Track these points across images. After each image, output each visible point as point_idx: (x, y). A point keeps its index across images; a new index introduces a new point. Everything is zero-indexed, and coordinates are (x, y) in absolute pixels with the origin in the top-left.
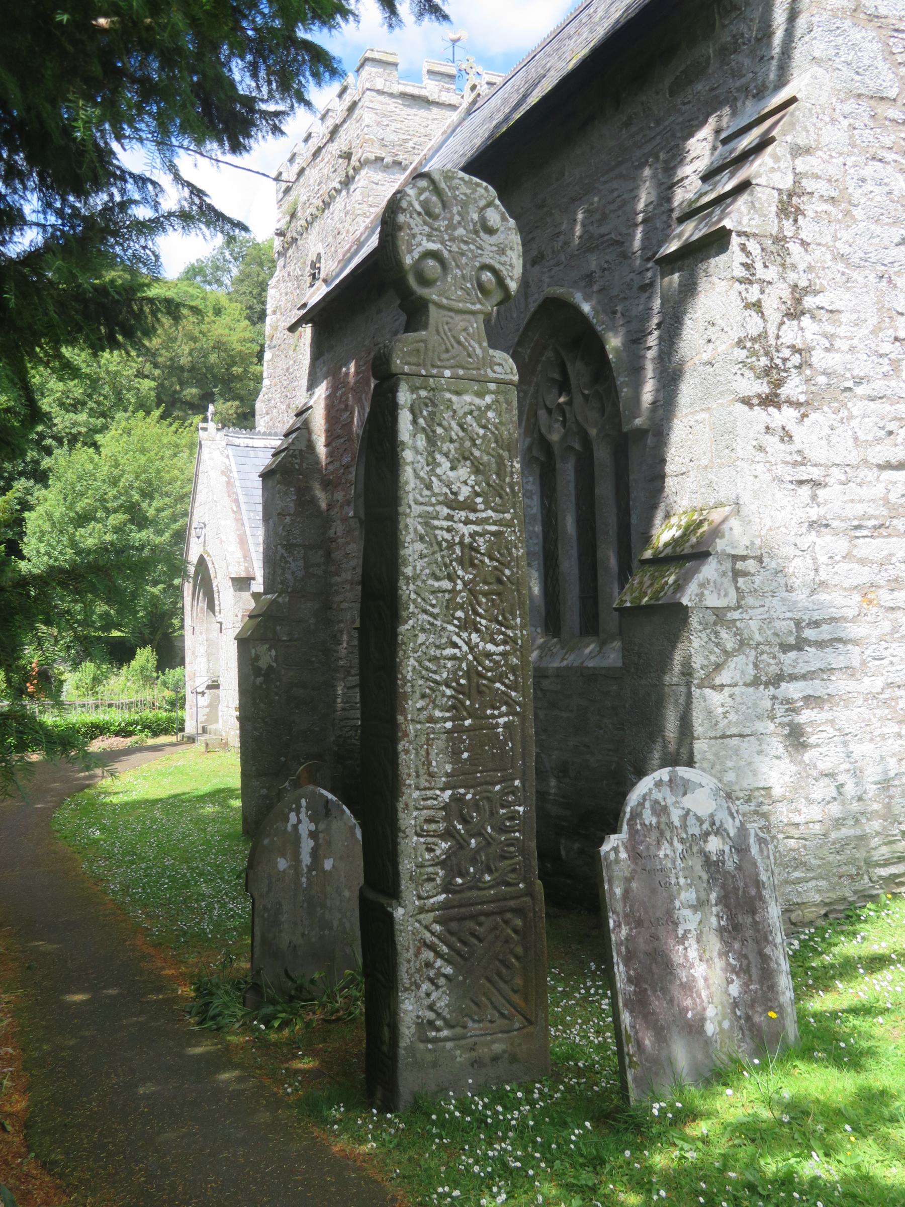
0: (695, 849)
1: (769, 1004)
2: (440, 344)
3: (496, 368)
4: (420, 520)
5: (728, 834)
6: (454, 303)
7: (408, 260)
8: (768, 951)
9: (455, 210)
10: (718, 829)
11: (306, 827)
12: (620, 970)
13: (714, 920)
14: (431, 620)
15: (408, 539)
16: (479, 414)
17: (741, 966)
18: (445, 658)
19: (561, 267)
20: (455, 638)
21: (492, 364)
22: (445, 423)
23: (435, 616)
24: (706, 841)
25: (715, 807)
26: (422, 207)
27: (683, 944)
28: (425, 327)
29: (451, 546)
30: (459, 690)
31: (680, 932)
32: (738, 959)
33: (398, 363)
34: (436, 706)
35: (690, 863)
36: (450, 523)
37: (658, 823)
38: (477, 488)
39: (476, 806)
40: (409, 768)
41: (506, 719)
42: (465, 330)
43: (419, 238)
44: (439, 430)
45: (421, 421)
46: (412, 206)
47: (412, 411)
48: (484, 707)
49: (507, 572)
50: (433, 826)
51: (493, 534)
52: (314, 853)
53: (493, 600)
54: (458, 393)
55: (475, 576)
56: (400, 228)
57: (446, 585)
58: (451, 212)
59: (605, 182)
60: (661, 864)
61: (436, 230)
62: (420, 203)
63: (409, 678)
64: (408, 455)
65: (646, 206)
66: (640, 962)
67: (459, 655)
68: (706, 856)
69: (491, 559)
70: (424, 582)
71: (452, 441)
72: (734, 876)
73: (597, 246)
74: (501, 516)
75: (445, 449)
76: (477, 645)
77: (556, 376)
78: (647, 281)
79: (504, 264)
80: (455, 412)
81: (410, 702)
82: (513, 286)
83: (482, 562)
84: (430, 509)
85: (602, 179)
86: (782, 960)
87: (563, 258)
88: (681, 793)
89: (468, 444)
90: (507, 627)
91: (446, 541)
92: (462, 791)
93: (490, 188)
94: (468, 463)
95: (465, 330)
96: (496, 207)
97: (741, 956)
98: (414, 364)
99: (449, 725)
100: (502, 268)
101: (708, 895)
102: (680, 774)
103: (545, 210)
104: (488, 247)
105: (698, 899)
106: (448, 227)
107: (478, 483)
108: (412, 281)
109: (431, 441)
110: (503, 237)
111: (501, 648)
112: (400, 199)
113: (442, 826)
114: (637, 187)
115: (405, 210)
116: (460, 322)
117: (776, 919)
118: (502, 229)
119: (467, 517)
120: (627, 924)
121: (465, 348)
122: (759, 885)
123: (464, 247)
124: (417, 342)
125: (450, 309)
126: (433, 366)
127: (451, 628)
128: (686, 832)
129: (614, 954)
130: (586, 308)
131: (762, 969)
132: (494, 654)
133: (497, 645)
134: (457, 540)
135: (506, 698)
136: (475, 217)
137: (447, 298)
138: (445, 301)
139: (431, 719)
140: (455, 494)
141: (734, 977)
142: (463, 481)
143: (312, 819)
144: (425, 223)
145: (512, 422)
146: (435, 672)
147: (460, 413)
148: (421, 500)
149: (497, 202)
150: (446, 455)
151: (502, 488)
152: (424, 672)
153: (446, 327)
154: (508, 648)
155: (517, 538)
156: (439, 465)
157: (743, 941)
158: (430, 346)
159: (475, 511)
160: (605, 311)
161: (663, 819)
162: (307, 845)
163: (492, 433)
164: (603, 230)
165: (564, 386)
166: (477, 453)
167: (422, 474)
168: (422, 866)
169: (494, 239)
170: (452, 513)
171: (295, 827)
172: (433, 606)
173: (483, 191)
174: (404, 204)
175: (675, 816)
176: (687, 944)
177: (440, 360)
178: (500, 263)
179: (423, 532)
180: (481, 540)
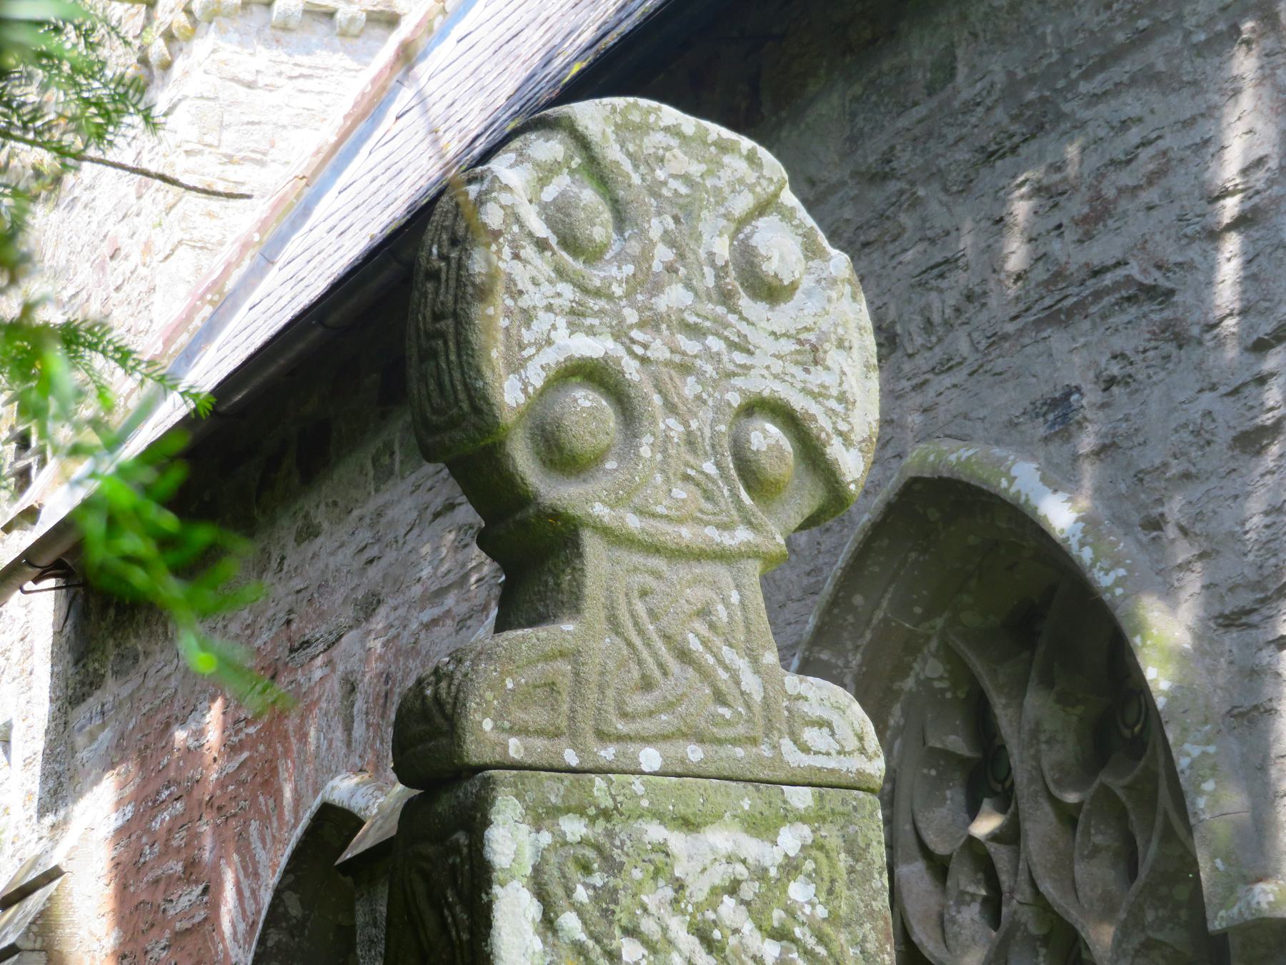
3: (811, 735)
7: (510, 394)
9: (655, 228)
19: (959, 376)
21: (795, 724)
22: (648, 926)
26: (550, 222)
28: (573, 604)
33: (486, 732)
42: (704, 613)
43: (543, 321)
45: (570, 922)
46: (518, 220)
54: (688, 824)
56: (483, 293)
58: (643, 232)
59: (1096, 98)
61: (597, 293)
62: (544, 207)
65: (1245, 172)
73: (1081, 305)
77: (957, 743)
78: (1268, 419)
79: (818, 395)
80: (680, 886)
82: (852, 465)
85: (1084, 87)
87: (964, 347)
93: (764, 153)
96: (787, 215)
98: (540, 733)
100: (814, 408)
103: (893, 186)
104: (768, 345)
106: (633, 285)
108: (523, 459)
110: (812, 306)
112: (480, 201)
114: (1211, 113)
115: (496, 234)
116: (688, 587)
118: (807, 282)
123: (690, 346)
124: (547, 658)
125: (654, 549)
130: (1060, 515)
136: (722, 248)
138: (633, 523)
144: (561, 273)
145: (872, 914)
147: (699, 890)
149: (789, 198)
158: (591, 673)
160: (1120, 521)
163: (807, 953)
164: (1099, 252)
165: (985, 777)
169: (784, 316)
173: (742, 166)
174: (493, 216)
177: (624, 715)
178: (805, 391)
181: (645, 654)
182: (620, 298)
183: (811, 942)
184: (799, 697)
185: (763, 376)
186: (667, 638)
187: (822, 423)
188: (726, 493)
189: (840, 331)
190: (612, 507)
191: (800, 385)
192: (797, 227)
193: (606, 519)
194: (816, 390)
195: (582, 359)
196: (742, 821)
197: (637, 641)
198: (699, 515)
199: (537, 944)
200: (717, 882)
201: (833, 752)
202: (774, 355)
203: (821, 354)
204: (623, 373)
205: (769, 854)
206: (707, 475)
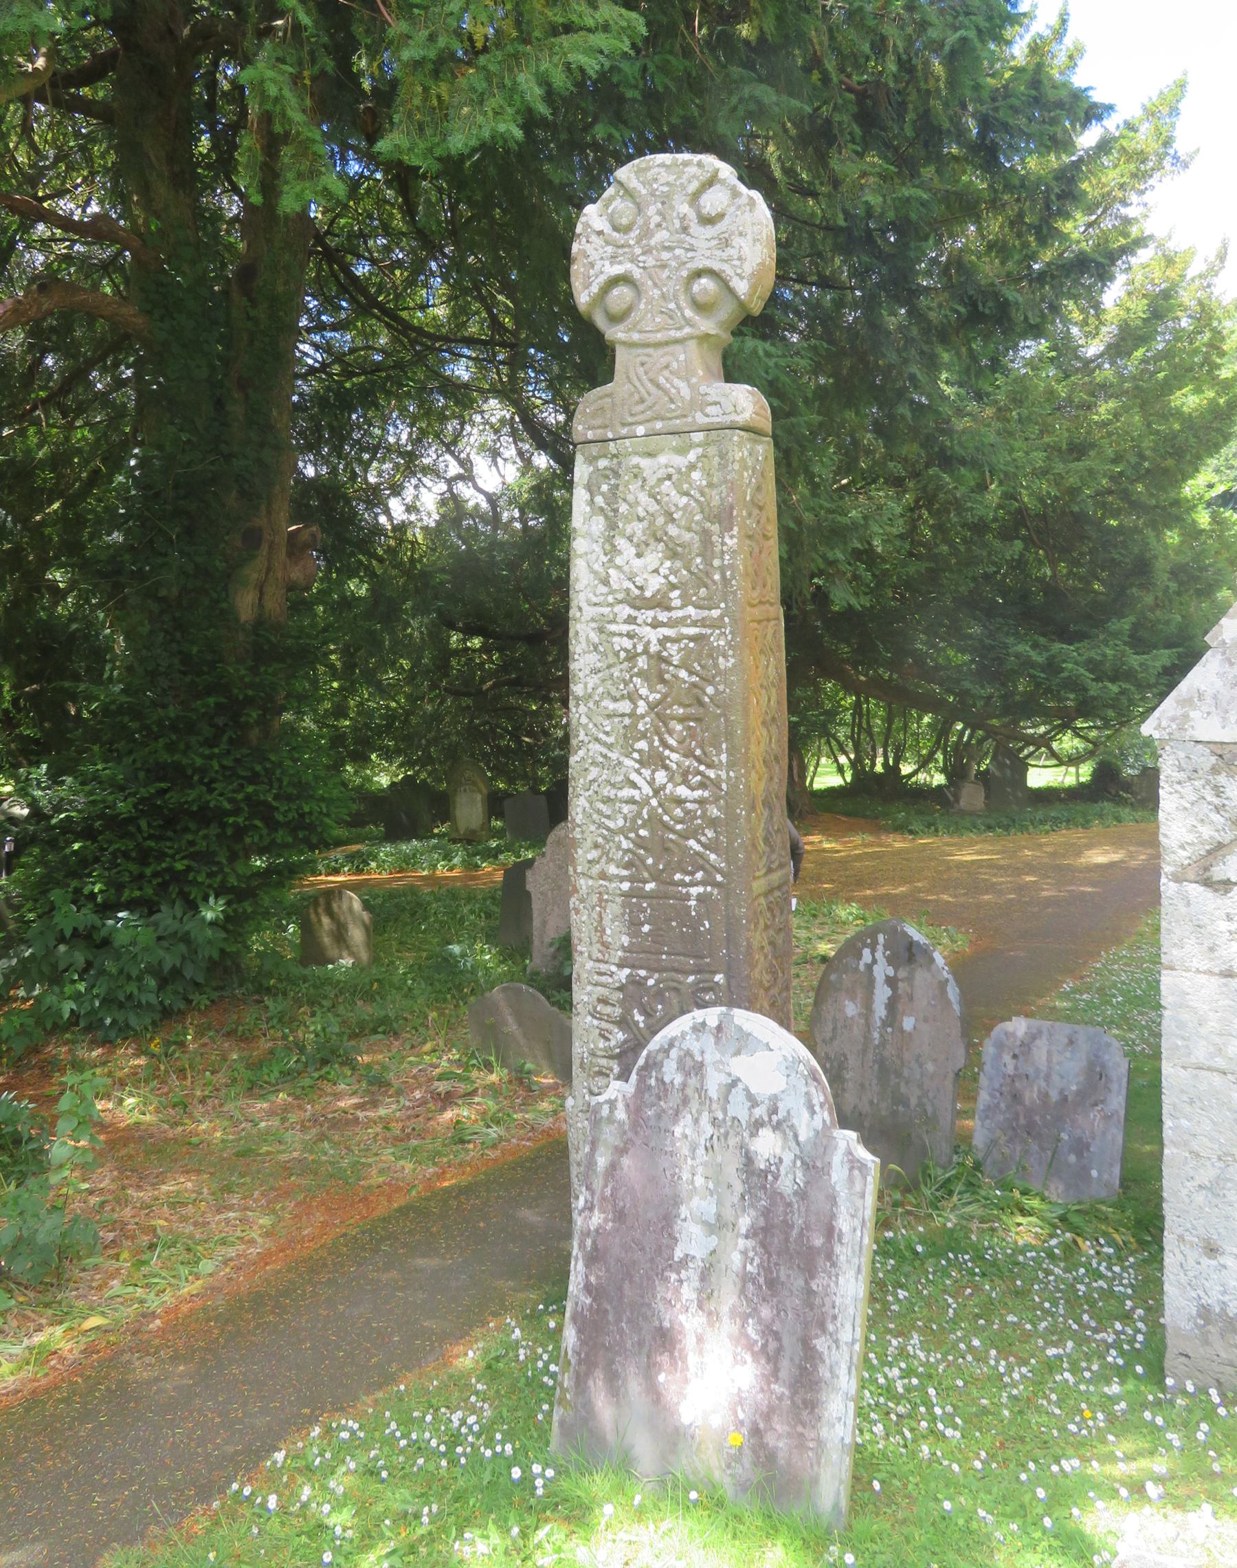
0: (733, 1141)
1: (800, 1429)
2: (632, 395)
4: (594, 625)
5: (796, 1136)
7: (583, 299)
8: (821, 1344)
9: (651, 210)
10: (779, 1123)
11: (882, 970)
12: (578, 1269)
13: (736, 1258)
14: (605, 751)
15: (578, 650)
16: (679, 478)
17: (765, 1346)
18: (621, 801)
20: (634, 777)
22: (630, 498)
23: (610, 747)
24: (754, 1134)
25: (784, 1086)
27: (679, 1273)
28: (609, 377)
29: (632, 657)
30: (640, 843)
31: (678, 1254)
32: (763, 1334)
34: (609, 860)
35: (719, 1159)
36: (632, 627)
37: (684, 1085)
38: (672, 578)
39: (659, 995)
40: (580, 931)
41: (701, 889)
44: (623, 508)
47: (589, 487)
48: (671, 868)
49: (710, 690)
50: (608, 1010)
51: (692, 638)
52: (892, 1005)
53: (690, 728)
54: (650, 455)
55: (665, 696)
57: (625, 706)
60: (673, 1144)
61: (623, 246)
63: (578, 821)
64: (579, 545)
66: (607, 1271)
67: (637, 798)
68: (749, 1160)
69: (691, 673)
70: (597, 703)
71: (640, 520)
72: (790, 1205)
74: (706, 613)
75: (629, 531)
76: (664, 787)
81: (580, 851)
83: (675, 676)
84: (606, 610)
86: (843, 1371)
88: (732, 1050)
89: (660, 520)
90: (709, 766)
91: (626, 650)
92: (643, 973)
94: (661, 546)
95: (667, 367)
97: (768, 1331)
99: (626, 886)
101: (737, 1217)
102: (737, 1021)
104: (706, 245)
105: (719, 1216)
107: (673, 571)
108: (600, 321)
109: (612, 526)
111: (698, 794)
113: (618, 1011)
117: (848, 1301)
119: (655, 618)
120: (603, 1211)
121: (666, 392)
122: (830, 1232)
123: (665, 255)
125: (647, 345)
126: (624, 425)
127: (628, 762)
128: (725, 1111)
129: (575, 1244)
131: (803, 1369)
132: (685, 801)
133: (693, 789)
134: (640, 649)
135: (701, 862)
136: (685, 209)
137: (640, 332)
138: (636, 337)
139: (603, 876)
140: (641, 588)
141: (748, 1358)
142: (651, 570)
143: (890, 961)
144: (607, 243)
146: (608, 817)
147: (652, 481)
148: (595, 600)
150: (630, 539)
151: (707, 574)
152: (595, 816)
153: (641, 370)
154: (706, 794)
155: (728, 643)
156: (620, 553)
157: (780, 1310)
159: (669, 609)
161: (693, 1081)
162: (882, 993)
163: (696, 500)
166: (673, 530)
167: (596, 567)
168: (593, 1054)
170: (634, 613)
171: (869, 967)
172: (607, 733)
175: (714, 1082)
176: (684, 1274)
179: (596, 640)
180: (673, 649)
183: (698, 495)
186: (651, 381)
187: (728, 270)
197: (638, 384)
199: (588, 509)
205: (681, 461)
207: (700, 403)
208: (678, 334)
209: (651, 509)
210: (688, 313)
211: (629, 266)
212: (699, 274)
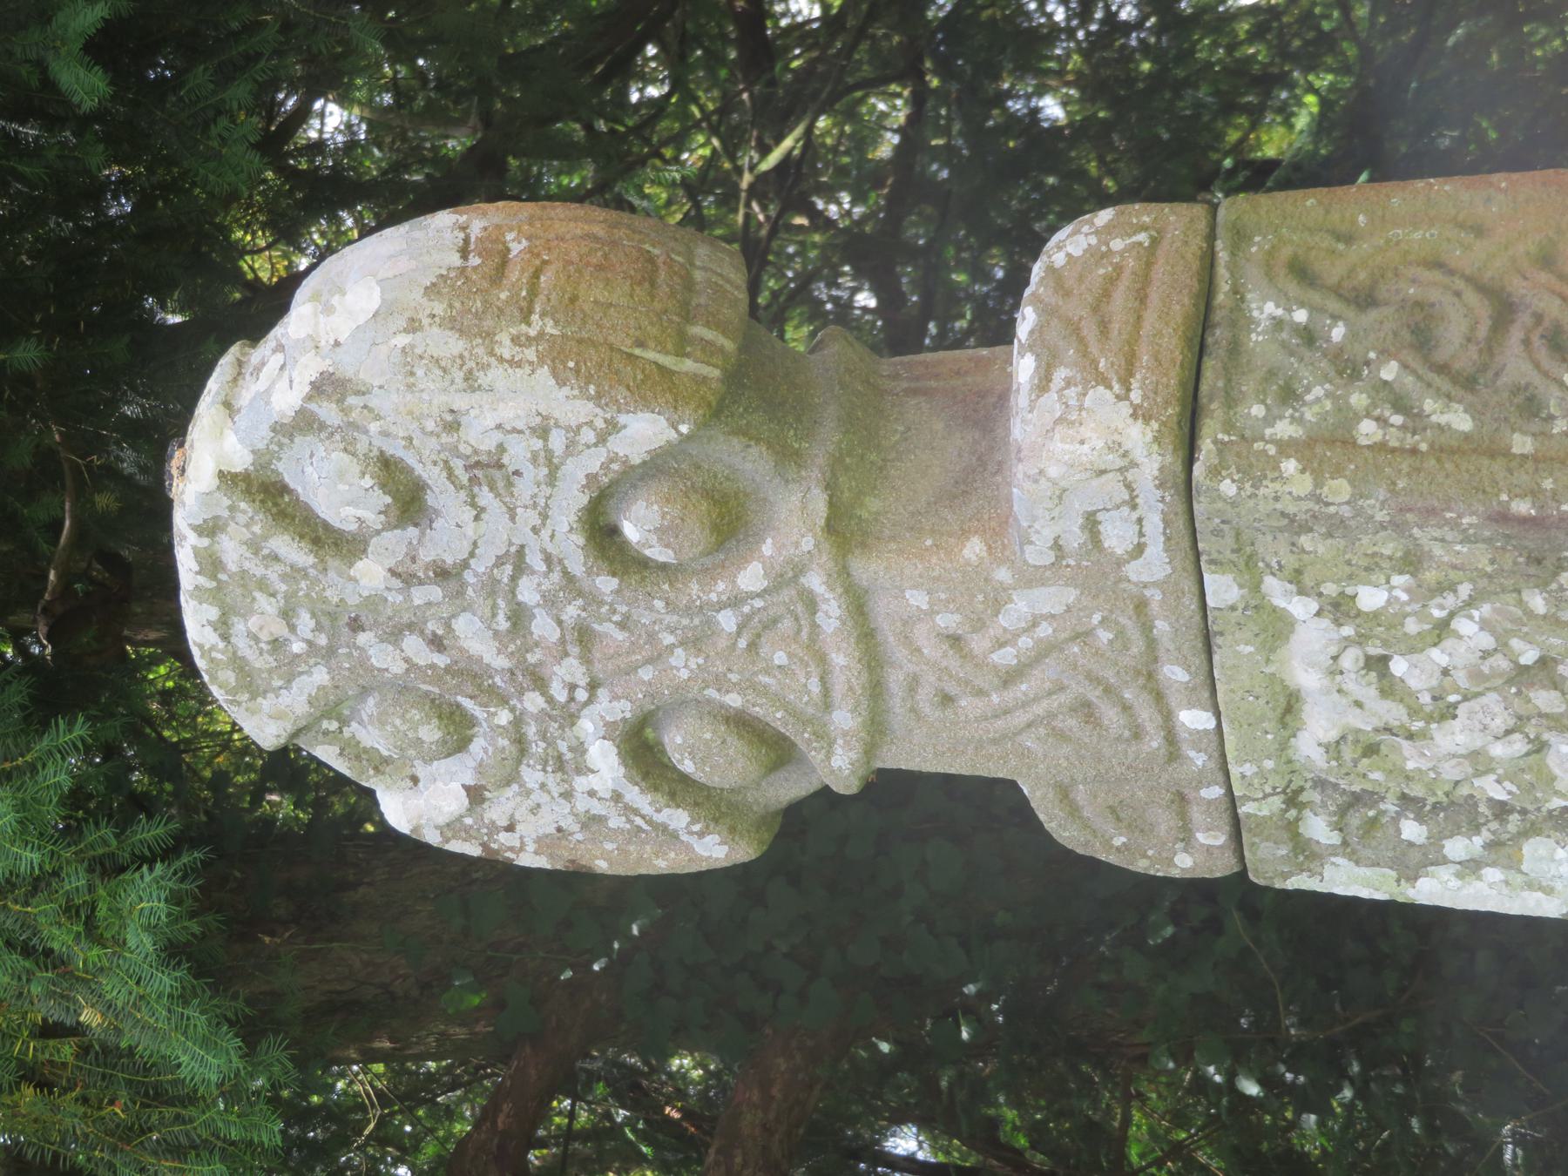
6: (839, 689)
54: (1289, 707)
125: (876, 690)
136: (371, 573)
137: (827, 704)
138: (844, 719)
177: (1137, 734)
181: (1039, 709)
182: (512, 710)
183: (1450, 601)
184: (1057, 546)
185: (552, 536)
188: (758, 603)
189: (430, 425)
190: (831, 744)
191: (549, 491)
192: (281, 445)
193: (853, 755)
194: (545, 471)
195: (624, 763)
196: (1273, 650)
197: (1020, 718)
198: (804, 634)
200: (1373, 692)
201: (1135, 515)
202: (513, 519)
203: (484, 458)
204: (624, 720)
206: (741, 628)
207: (1090, 564)
208: (832, 613)
209: (1500, 722)
210: (751, 578)
211: (587, 726)
212: (601, 532)
